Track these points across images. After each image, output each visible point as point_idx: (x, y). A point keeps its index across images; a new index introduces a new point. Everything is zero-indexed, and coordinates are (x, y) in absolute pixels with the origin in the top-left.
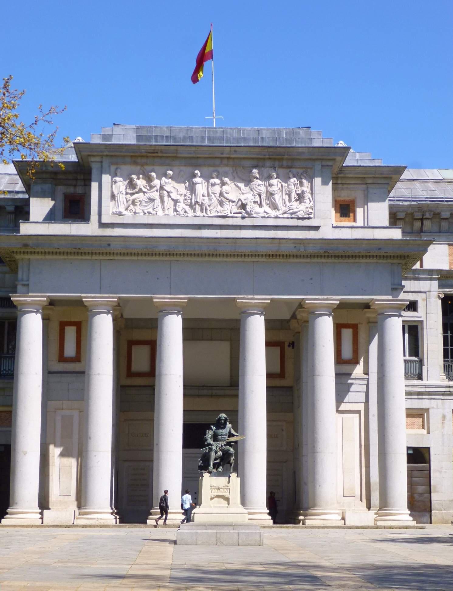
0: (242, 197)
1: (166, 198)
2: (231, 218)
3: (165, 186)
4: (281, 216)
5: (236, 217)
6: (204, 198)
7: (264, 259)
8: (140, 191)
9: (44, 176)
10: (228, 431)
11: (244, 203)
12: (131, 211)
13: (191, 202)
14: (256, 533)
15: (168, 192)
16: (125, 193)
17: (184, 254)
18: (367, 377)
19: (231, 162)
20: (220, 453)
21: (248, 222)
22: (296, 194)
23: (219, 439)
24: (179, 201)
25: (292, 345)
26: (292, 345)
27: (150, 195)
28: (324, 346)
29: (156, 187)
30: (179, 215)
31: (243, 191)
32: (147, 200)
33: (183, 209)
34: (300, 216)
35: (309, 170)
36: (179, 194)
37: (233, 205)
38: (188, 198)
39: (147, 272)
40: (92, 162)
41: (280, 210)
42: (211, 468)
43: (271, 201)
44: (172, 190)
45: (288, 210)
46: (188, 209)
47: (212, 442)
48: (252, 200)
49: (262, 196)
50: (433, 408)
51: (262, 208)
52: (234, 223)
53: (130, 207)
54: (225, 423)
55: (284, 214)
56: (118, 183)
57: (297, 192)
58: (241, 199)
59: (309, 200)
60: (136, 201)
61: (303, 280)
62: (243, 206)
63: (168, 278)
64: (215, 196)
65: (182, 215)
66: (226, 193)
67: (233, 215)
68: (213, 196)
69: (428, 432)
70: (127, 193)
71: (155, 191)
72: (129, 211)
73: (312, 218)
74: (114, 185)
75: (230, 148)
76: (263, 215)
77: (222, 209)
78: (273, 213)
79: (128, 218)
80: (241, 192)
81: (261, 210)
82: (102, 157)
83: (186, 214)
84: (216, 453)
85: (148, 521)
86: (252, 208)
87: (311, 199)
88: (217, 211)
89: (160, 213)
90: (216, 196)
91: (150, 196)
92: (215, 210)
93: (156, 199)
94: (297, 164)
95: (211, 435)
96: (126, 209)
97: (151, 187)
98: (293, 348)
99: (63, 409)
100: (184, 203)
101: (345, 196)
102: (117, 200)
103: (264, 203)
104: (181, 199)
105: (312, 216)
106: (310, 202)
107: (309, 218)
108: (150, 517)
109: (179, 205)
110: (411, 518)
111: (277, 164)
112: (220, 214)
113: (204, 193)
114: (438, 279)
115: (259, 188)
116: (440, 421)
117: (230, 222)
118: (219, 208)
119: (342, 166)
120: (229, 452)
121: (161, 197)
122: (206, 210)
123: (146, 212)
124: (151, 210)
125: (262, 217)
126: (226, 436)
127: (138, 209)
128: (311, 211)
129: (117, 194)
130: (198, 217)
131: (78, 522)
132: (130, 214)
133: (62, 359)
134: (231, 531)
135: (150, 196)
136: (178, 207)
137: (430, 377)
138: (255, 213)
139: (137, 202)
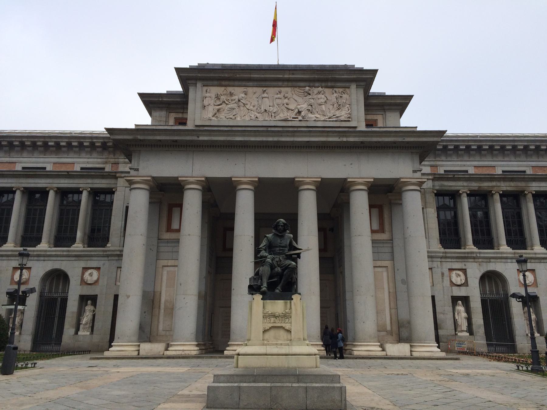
0: (299, 107)
1: (242, 108)
2: (290, 122)
4: (328, 120)
5: (294, 121)
6: (270, 108)
8: (224, 102)
9: (161, 106)
10: (288, 242)
14: (334, 387)
17: (255, 146)
18: (392, 242)
19: (290, 84)
20: (278, 269)
21: (303, 124)
22: (338, 105)
23: (277, 251)
25: (332, 230)
26: (332, 230)
28: (362, 213)
31: (299, 104)
34: (341, 120)
35: (347, 89)
38: (259, 108)
39: (228, 160)
42: (264, 287)
44: (247, 102)
45: (333, 115)
46: (258, 115)
47: (267, 254)
50: (435, 267)
51: (313, 114)
54: (285, 230)
55: (329, 118)
57: (339, 104)
59: (347, 109)
60: (221, 110)
61: (345, 165)
62: (299, 112)
63: (243, 164)
67: (291, 119)
69: (433, 286)
73: (350, 121)
74: (204, 100)
76: (314, 119)
79: (215, 122)
84: (272, 267)
85: (225, 352)
87: (349, 108)
89: (238, 119)
92: (278, 116)
94: (339, 84)
95: (265, 247)
98: (332, 232)
99: (168, 266)
101: (370, 117)
105: (351, 120)
106: (349, 110)
107: (349, 121)
108: (228, 348)
109: (252, 113)
110: (439, 350)
111: (323, 84)
114: (433, 180)
116: (441, 277)
117: (290, 124)
119: (368, 95)
120: (290, 266)
122: (272, 116)
123: (227, 117)
124: (231, 116)
126: (286, 249)
127: (222, 116)
131: (168, 353)
132: (216, 119)
133: (169, 229)
134: (294, 385)
137: (431, 246)
139: (221, 111)
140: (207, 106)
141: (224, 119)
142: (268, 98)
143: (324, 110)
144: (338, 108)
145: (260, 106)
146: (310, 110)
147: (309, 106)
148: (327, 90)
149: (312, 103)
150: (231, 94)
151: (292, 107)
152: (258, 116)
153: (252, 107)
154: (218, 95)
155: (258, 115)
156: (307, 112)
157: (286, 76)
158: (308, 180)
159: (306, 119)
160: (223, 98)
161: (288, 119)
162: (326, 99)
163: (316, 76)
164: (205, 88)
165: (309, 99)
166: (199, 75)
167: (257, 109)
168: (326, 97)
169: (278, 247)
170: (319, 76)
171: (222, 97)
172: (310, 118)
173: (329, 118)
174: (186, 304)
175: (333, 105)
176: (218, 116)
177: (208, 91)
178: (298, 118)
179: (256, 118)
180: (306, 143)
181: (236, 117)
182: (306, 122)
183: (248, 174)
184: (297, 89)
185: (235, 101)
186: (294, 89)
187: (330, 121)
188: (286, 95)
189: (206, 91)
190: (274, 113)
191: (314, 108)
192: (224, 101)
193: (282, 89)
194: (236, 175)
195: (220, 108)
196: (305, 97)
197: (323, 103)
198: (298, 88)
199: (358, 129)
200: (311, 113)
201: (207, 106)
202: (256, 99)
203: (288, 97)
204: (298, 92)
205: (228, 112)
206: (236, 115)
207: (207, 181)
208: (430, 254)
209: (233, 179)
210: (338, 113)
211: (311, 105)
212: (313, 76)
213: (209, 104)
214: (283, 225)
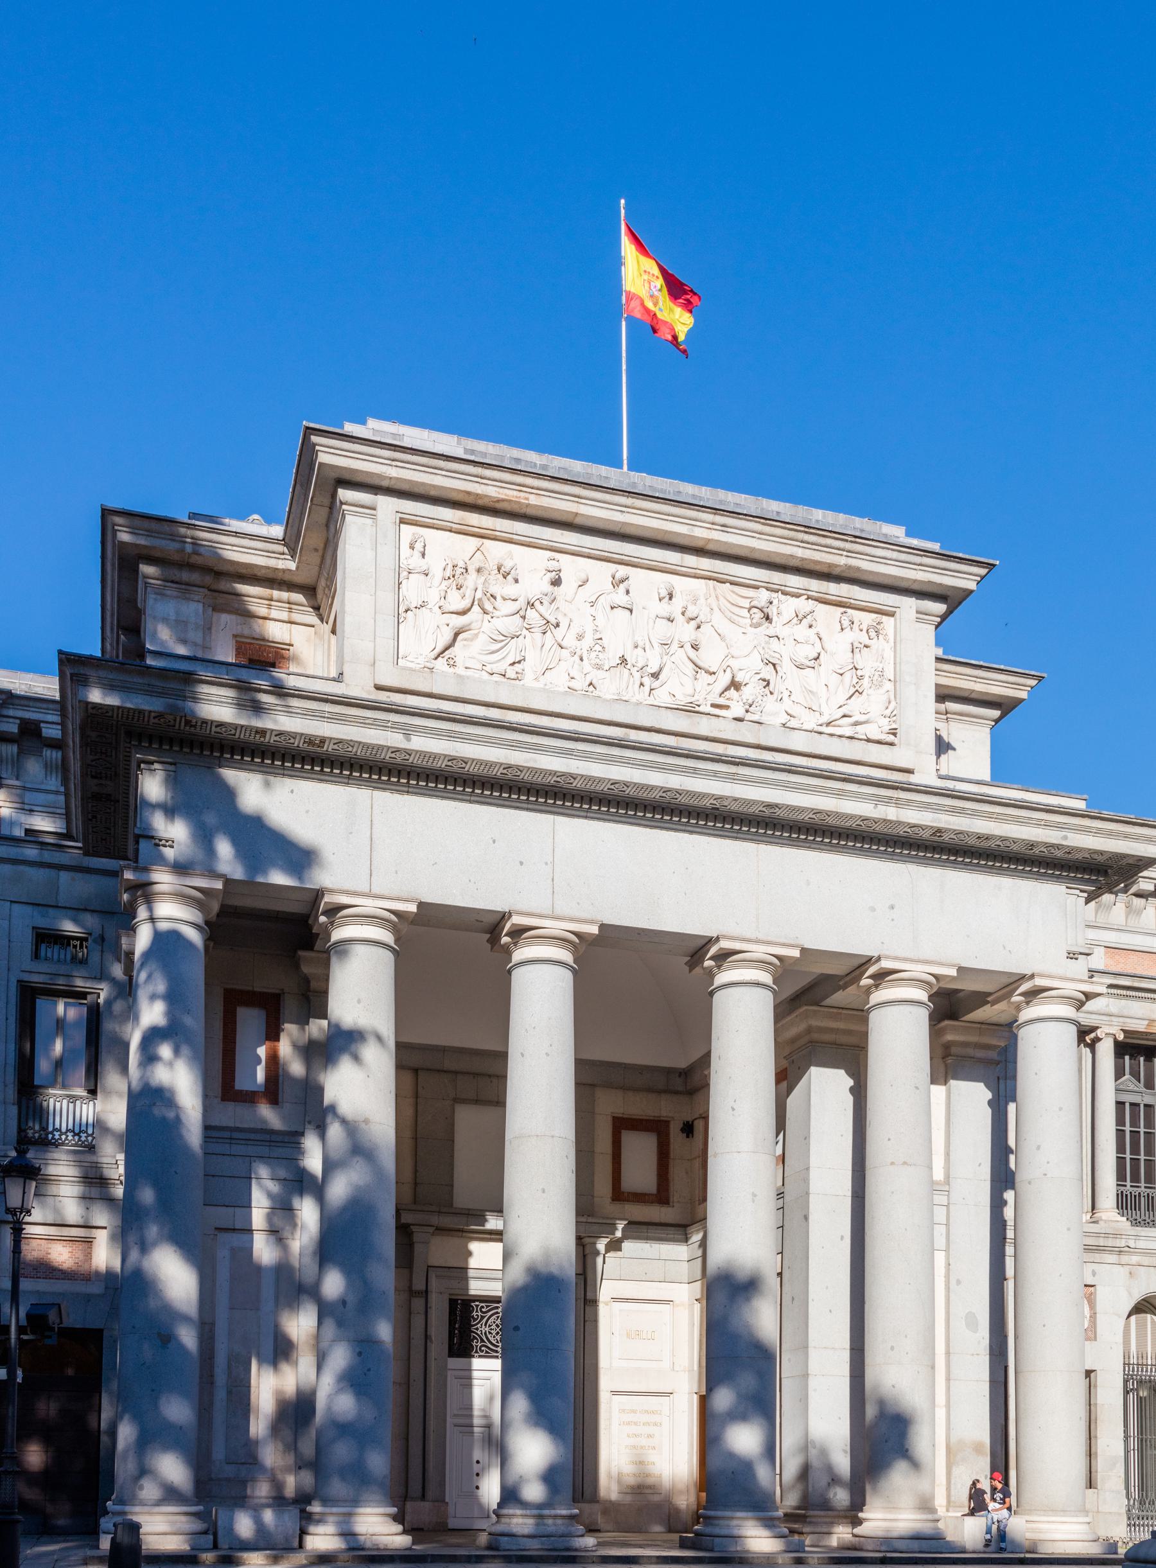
5: (718, 716)
11: (736, 679)
21: (745, 733)
35: (885, 618)
38: (598, 648)
45: (841, 714)
49: (778, 668)
55: (828, 724)
57: (859, 673)
63: (546, 864)
66: (695, 647)
67: (709, 709)
87: (892, 698)
105: (896, 741)
107: (892, 744)
117: (704, 726)
123: (488, 668)
128: (894, 726)
132: (446, 668)
143: (815, 691)
144: (857, 688)
145: (601, 639)
151: (710, 657)
153: (570, 641)
155: (595, 676)
161: (697, 709)
162: (818, 648)
173: (828, 724)
174: (365, 1374)
175: (841, 675)
178: (727, 707)
179: (589, 685)
183: (564, 907)
185: (514, 606)
187: (832, 735)
188: (692, 611)
189: (412, 547)
190: (655, 676)
194: (519, 907)
197: (811, 664)
198: (728, 584)
199: (914, 779)
201: (414, 610)
204: (730, 602)
206: (519, 662)
208: (1091, 1241)
210: (856, 706)
211: (774, 665)
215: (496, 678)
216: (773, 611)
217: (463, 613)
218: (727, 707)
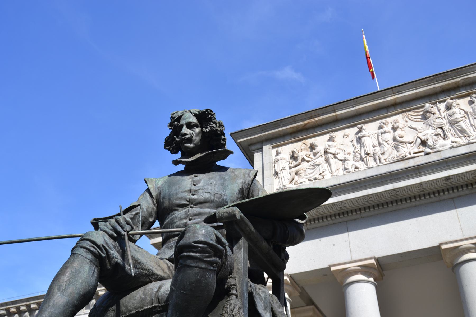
0: (420, 135)
2: (411, 160)
3: (329, 149)
5: (418, 156)
6: (375, 148)
7: (466, 191)
8: (303, 160)
12: (296, 183)
13: (361, 157)
15: (333, 154)
16: (288, 168)
21: (434, 158)
23: (178, 223)
24: (346, 159)
27: (314, 162)
29: (320, 153)
30: (349, 172)
31: (419, 131)
32: (313, 167)
33: (353, 165)
36: (346, 153)
37: (411, 147)
40: (253, 150)
41: (471, 136)
43: (458, 130)
44: (338, 151)
46: (358, 164)
48: (432, 134)
49: (443, 128)
52: (416, 163)
53: (294, 180)
56: (280, 161)
58: (419, 136)
60: (300, 172)
62: (424, 143)
63: (346, 241)
64: (388, 144)
65: (352, 171)
66: (400, 137)
67: (412, 155)
68: (385, 144)
70: (290, 168)
71: (319, 157)
72: (293, 184)
74: (276, 165)
75: (393, 90)
77: (398, 154)
78: (463, 141)
80: (417, 132)
81: (448, 143)
82: (262, 143)
83: (358, 169)
86: (434, 141)
88: (393, 157)
89: (328, 176)
90: (389, 143)
91: (314, 162)
92: (391, 156)
93: (321, 164)
96: (291, 182)
97: (315, 155)
100: (354, 160)
102: (280, 176)
103: (449, 134)
104: (350, 157)
109: (347, 163)
112: (396, 158)
113: (374, 144)
115: (438, 120)
117: (411, 163)
118: (395, 154)
121: (327, 161)
123: (312, 179)
124: (317, 176)
125: (451, 148)
129: (280, 171)
130: (372, 168)
135: (314, 162)
136: (347, 166)
138: (440, 147)
140: (280, 172)
141: (308, 182)
142: (369, 136)
143: (464, 127)
145: (359, 151)
146: (440, 135)
147: (437, 129)
148: (459, 101)
149: (441, 124)
150: (312, 147)
152: (358, 166)
153: (347, 156)
154: (294, 153)
155: (358, 164)
156: (435, 138)
157: (388, 99)
158: (465, 244)
159: (436, 150)
160: (301, 155)
161: (406, 157)
162: (462, 112)
163: (437, 85)
164: (275, 150)
165: (434, 120)
166: (264, 134)
167: (355, 156)
168: (463, 110)
169: (183, 206)
170: (441, 84)
171: (300, 154)
172: (443, 146)
176: (297, 181)
177: (279, 151)
178: (422, 151)
179: (355, 169)
180: (444, 182)
181: (324, 175)
182: (438, 153)
184: (410, 113)
186: (406, 114)
188: (396, 125)
190: (383, 154)
191: (446, 130)
192: (303, 158)
193: (389, 120)
195: (298, 169)
196: (428, 120)
197: (461, 119)
200: (444, 139)
202: (351, 144)
203: (401, 126)
205: (312, 171)
206: (323, 172)
207: (295, 282)
209: (332, 269)
212: (432, 87)
213: (283, 169)
214: (194, 120)
215: (314, 181)
216: (435, 110)
217: (299, 164)
218: (422, 151)
